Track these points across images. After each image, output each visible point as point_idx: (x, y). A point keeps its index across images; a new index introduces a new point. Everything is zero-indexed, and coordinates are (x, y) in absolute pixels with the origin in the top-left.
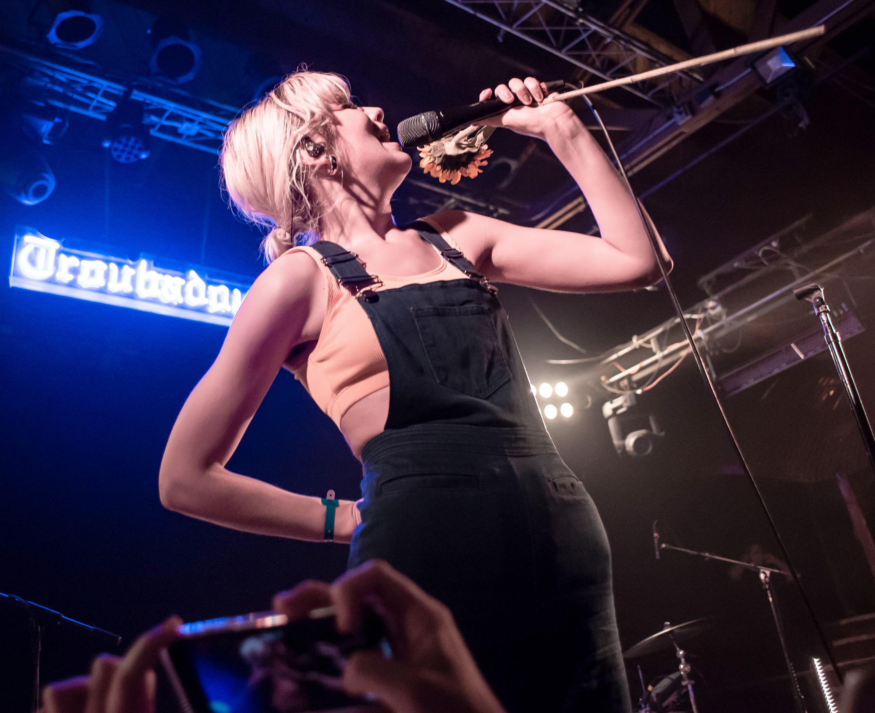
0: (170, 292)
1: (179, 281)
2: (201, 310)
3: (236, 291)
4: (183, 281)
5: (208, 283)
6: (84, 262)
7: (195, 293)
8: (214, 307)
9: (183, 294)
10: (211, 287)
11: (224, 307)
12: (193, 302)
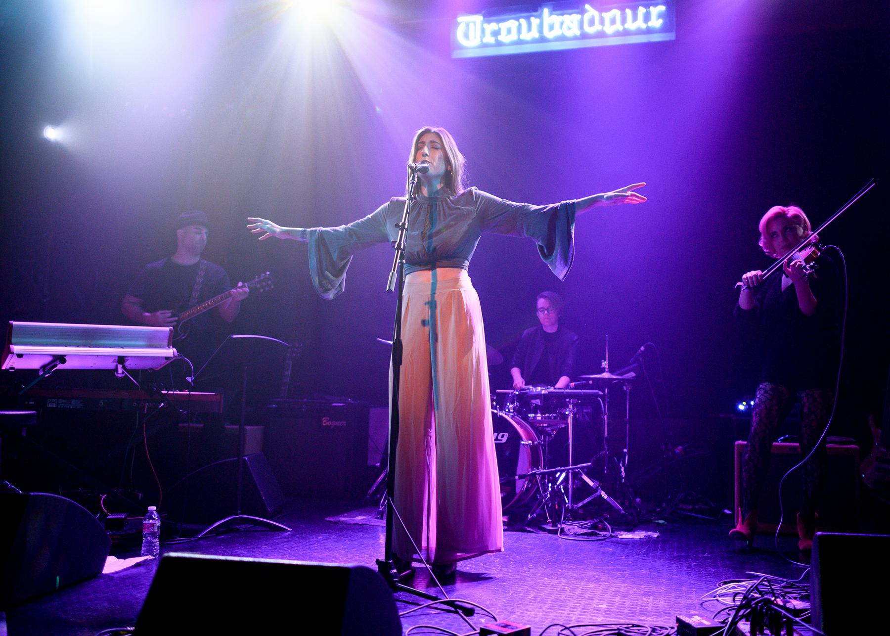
0: (570, 29)
1: (576, 17)
3: (628, 12)
4: (579, 17)
5: (601, 11)
7: (592, 23)
10: (604, 14)
11: (619, 27)
12: (590, 30)
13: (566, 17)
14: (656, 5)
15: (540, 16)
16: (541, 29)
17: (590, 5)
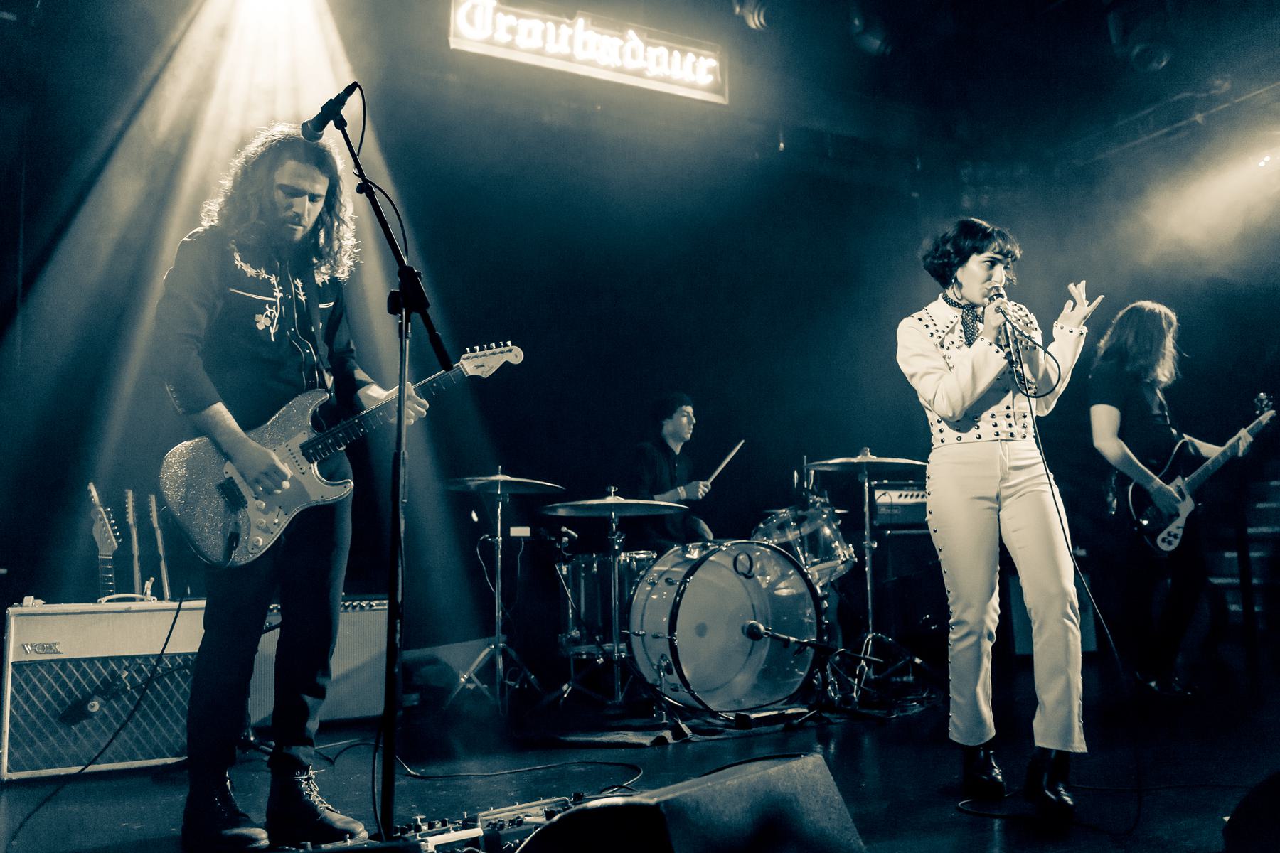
1: (617, 42)
2: (639, 74)
3: (676, 53)
4: (620, 42)
5: (647, 44)
6: (522, 21)
7: (634, 55)
8: (653, 71)
9: (621, 56)
10: (650, 49)
11: (663, 71)
12: (631, 64)
13: (606, 37)
14: (706, 57)
15: (570, 26)
16: (571, 40)
17: (635, 32)
